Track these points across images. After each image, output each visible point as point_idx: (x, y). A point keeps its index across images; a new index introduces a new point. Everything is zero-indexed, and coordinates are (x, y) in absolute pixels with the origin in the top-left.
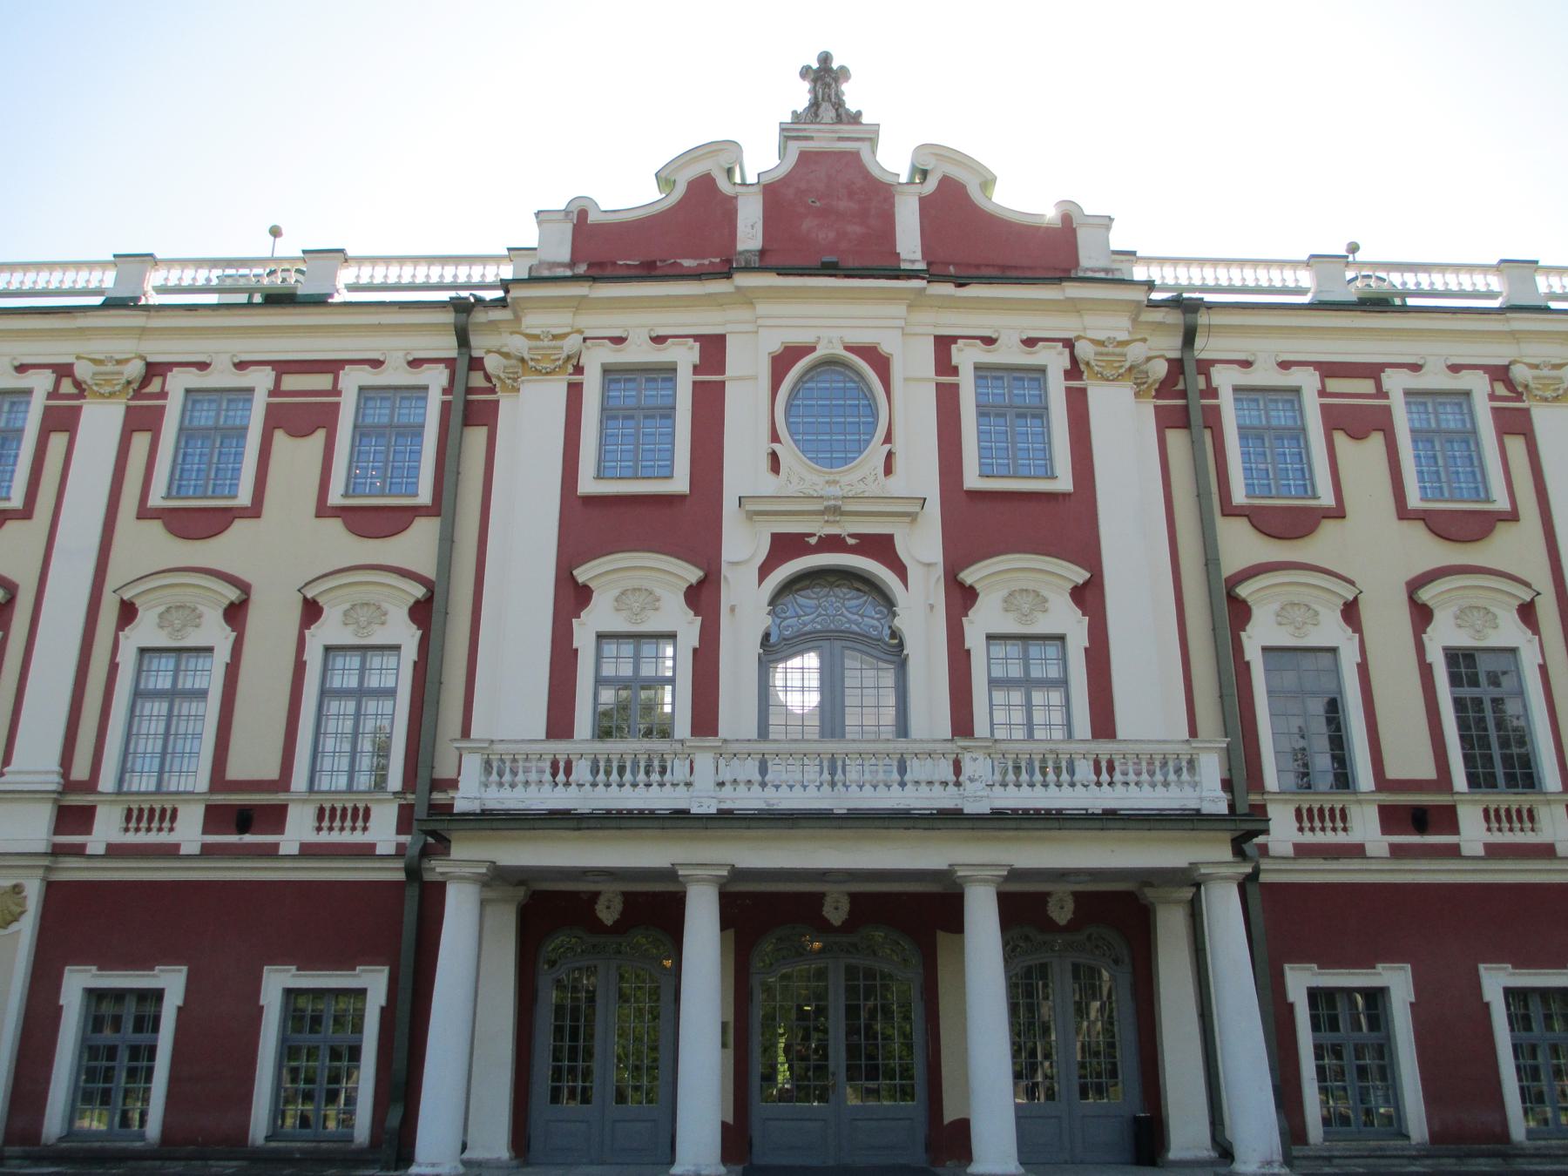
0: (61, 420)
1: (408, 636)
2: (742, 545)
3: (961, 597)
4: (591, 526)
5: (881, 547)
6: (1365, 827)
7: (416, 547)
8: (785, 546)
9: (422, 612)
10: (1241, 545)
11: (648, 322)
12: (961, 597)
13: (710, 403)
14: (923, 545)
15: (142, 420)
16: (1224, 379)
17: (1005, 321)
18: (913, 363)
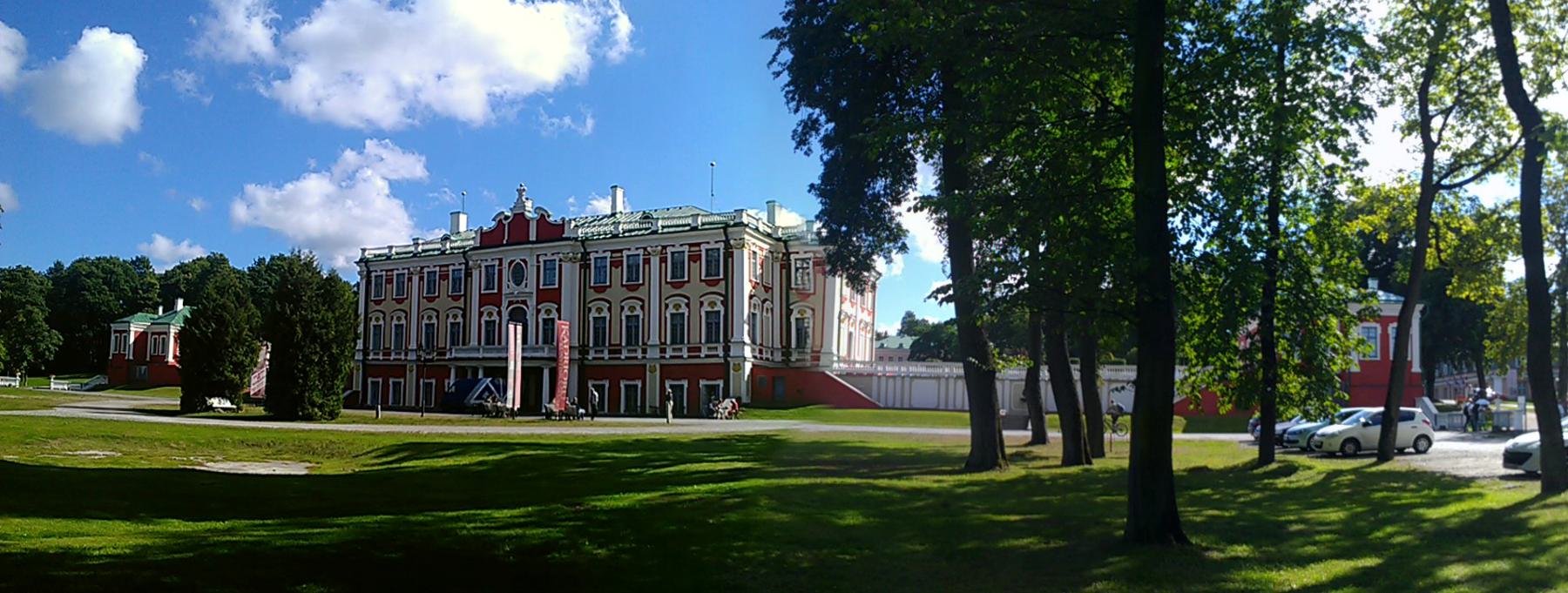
0: (410, 279)
1: (460, 319)
2: (505, 304)
3: (538, 311)
4: (484, 301)
5: (524, 302)
6: (606, 355)
7: (461, 303)
8: (510, 303)
9: (464, 316)
10: (592, 295)
11: (490, 256)
12: (538, 311)
13: (500, 272)
14: (532, 302)
15: (421, 279)
16: (592, 256)
17: (548, 250)
18: (532, 262)
